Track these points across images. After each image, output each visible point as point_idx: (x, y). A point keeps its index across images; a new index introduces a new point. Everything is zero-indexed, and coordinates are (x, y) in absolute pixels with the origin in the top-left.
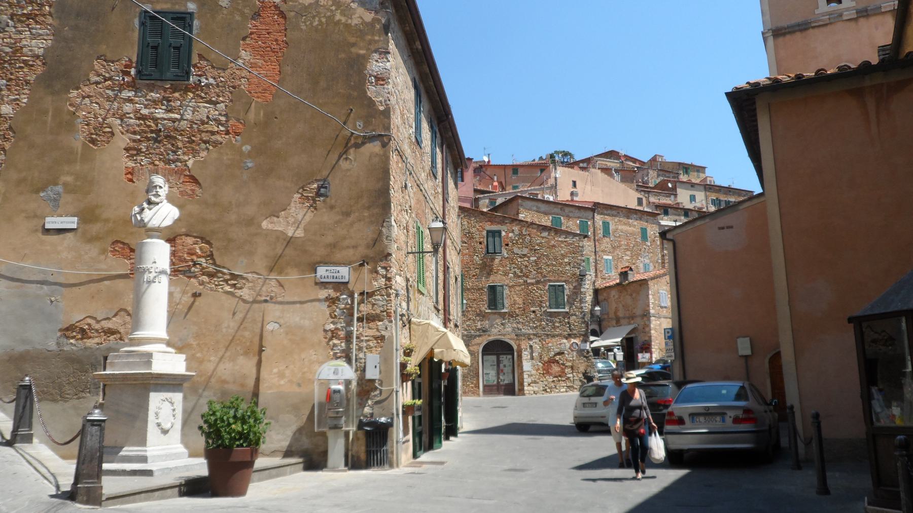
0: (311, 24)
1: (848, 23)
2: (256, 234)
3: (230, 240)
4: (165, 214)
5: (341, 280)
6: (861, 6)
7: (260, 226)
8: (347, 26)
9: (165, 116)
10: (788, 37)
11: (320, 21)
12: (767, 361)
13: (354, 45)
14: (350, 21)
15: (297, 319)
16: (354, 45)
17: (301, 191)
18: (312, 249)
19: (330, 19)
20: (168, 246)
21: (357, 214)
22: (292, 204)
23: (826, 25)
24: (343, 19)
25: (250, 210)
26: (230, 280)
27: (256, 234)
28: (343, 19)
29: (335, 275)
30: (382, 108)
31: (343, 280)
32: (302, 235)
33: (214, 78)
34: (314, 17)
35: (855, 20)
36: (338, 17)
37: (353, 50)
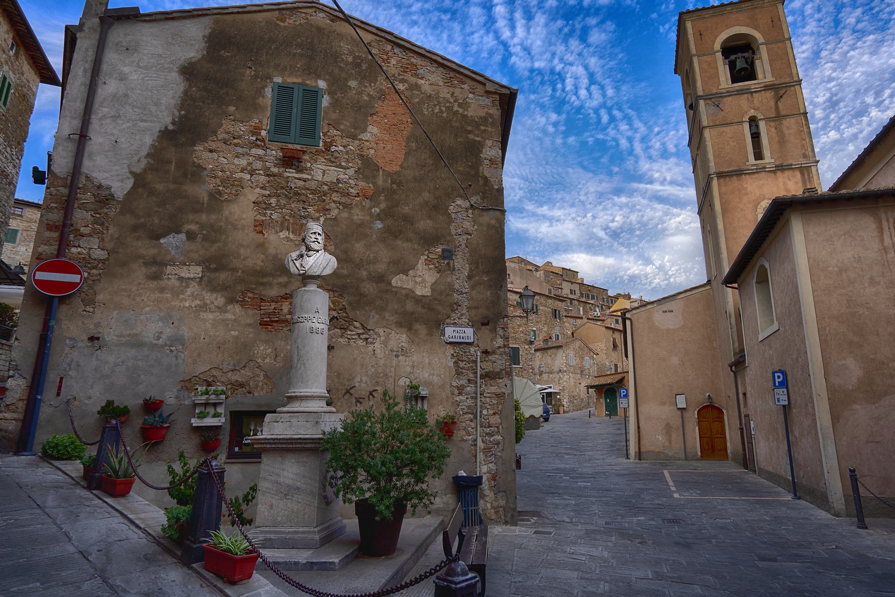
0: (433, 110)
1: (769, 174)
2: (387, 291)
3: (362, 295)
4: (320, 261)
5: (467, 341)
6: (778, 163)
7: (390, 284)
8: (465, 117)
9: (297, 176)
10: (728, 179)
11: (440, 109)
12: (696, 412)
13: (470, 132)
14: (466, 113)
15: (426, 375)
16: (470, 132)
17: (426, 253)
18: (439, 308)
19: (450, 109)
20: (327, 295)
21: (477, 278)
22: (419, 265)
23: (754, 173)
24: (461, 111)
25: (381, 267)
26: (363, 334)
27: (387, 291)
28: (461, 111)
29: (462, 335)
30: (496, 187)
31: (469, 341)
32: (429, 294)
33: (344, 147)
34: (435, 105)
35: (774, 172)
36: (456, 108)
37: (471, 136)
